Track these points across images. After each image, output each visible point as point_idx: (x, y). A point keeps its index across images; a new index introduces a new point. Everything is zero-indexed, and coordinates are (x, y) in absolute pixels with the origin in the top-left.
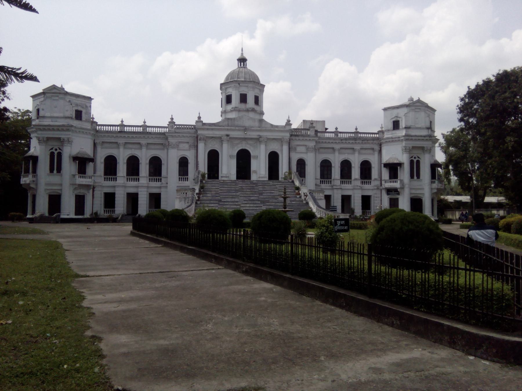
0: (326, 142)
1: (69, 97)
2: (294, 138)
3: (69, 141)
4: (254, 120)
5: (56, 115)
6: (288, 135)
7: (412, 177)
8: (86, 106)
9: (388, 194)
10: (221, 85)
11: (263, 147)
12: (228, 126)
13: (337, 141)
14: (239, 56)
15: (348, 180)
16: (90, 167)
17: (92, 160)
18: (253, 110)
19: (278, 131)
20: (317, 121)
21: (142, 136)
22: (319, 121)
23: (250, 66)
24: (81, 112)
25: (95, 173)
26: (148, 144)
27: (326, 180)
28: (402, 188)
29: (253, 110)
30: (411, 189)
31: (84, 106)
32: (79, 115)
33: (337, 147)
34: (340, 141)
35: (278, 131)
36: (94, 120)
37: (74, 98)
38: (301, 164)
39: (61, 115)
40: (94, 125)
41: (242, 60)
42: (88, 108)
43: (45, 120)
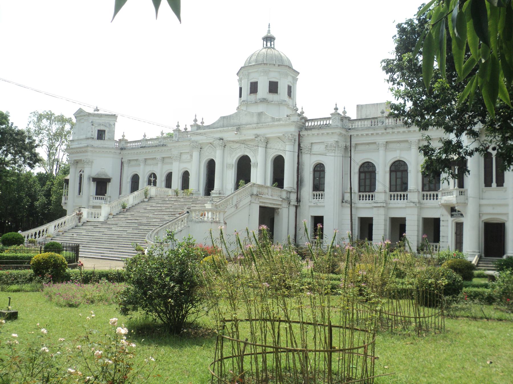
0: (362, 135)
1: (91, 118)
2: (304, 133)
3: (90, 163)
4: (252, 114)
5: (82, 137)
6: (293, 129)
7: (488, 183)
8: (110, 125)
9: (452, 215)
10: (237, 74)
11: (261, 150)
12: (223, 127)
13: (380, 132)
14: (265, 34)
15: (402, 193)
16: (111, 188)
17: (109, 180)
18: (264, 101)
19: (277, 126)
20: (377, 104)
21: (156, 149)
22: (381, 104)
23: (277, 44)
24: (105, 131)
25: (120, 194)
26: (164, 158)
27: (367, 194)
28: (465, 204)
29: (264, 101)
30: (480, 206)
31: (108, 125)
32: (101, 135)
33: (381, 140)
34: (384, 131)
35: (277, 126)
36: (126, 138)
37: (98, 118)
38: (319, 170)
39: (84, 137)
40: (123, 143)
41: (269, 39)
42: (112, 126)
43: (74, 143)
